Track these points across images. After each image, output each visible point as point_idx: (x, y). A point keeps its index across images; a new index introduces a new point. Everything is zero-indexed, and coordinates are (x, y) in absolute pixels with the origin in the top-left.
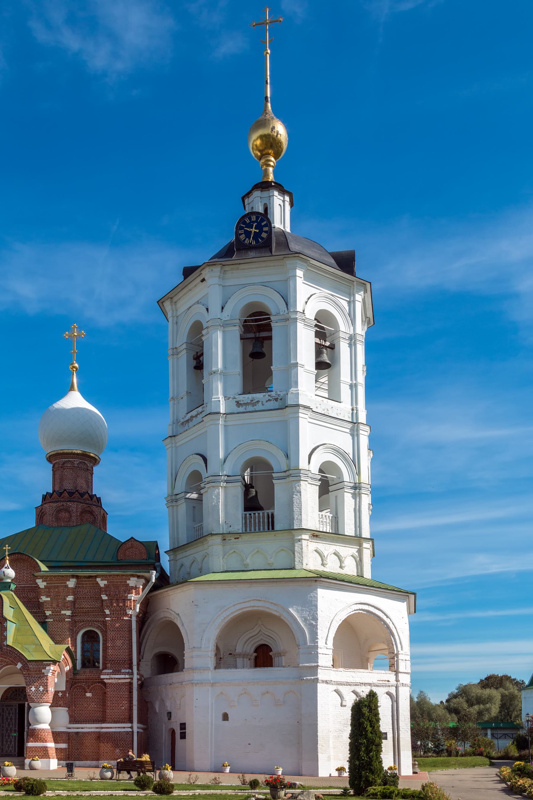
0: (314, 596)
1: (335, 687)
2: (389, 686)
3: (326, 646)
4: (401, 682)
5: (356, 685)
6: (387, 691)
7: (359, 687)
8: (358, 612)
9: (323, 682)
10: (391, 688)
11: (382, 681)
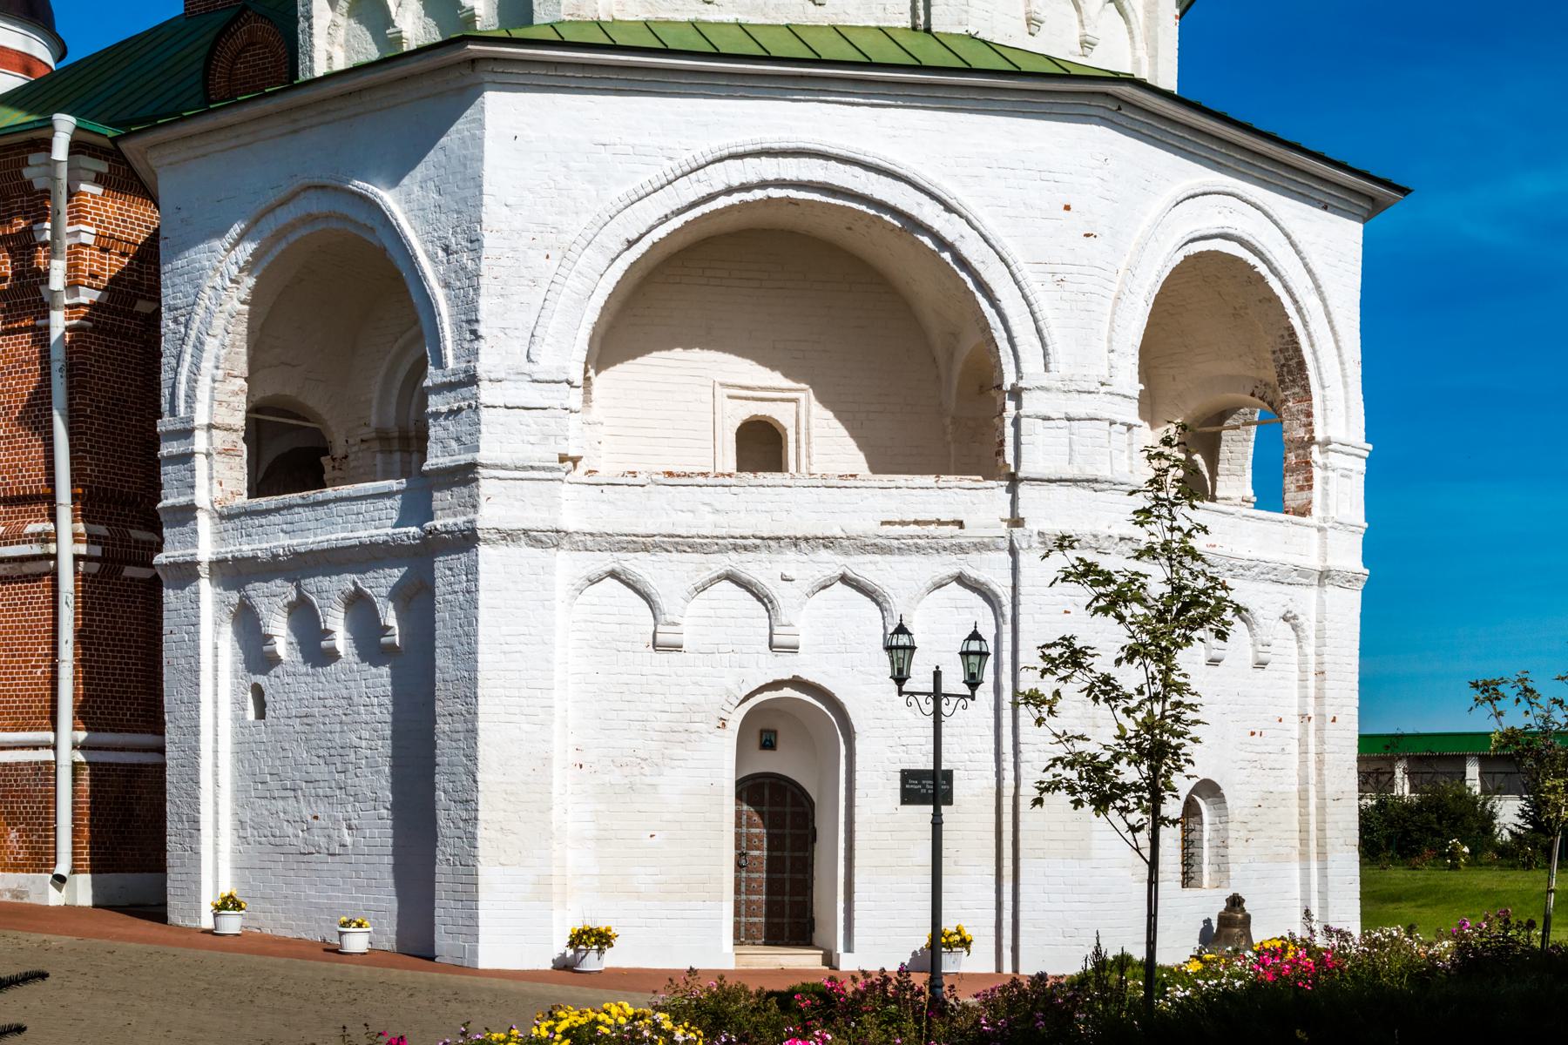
0: (473, 137)
1: (608, 561)
2: (962, 549)
3: (528, 368)
4: (1032, 526)
5: (740, 545)
6: (954, 571)
8: (759, 194)
9: (508, 536)
10: (974, 556)
11: (903, 523)
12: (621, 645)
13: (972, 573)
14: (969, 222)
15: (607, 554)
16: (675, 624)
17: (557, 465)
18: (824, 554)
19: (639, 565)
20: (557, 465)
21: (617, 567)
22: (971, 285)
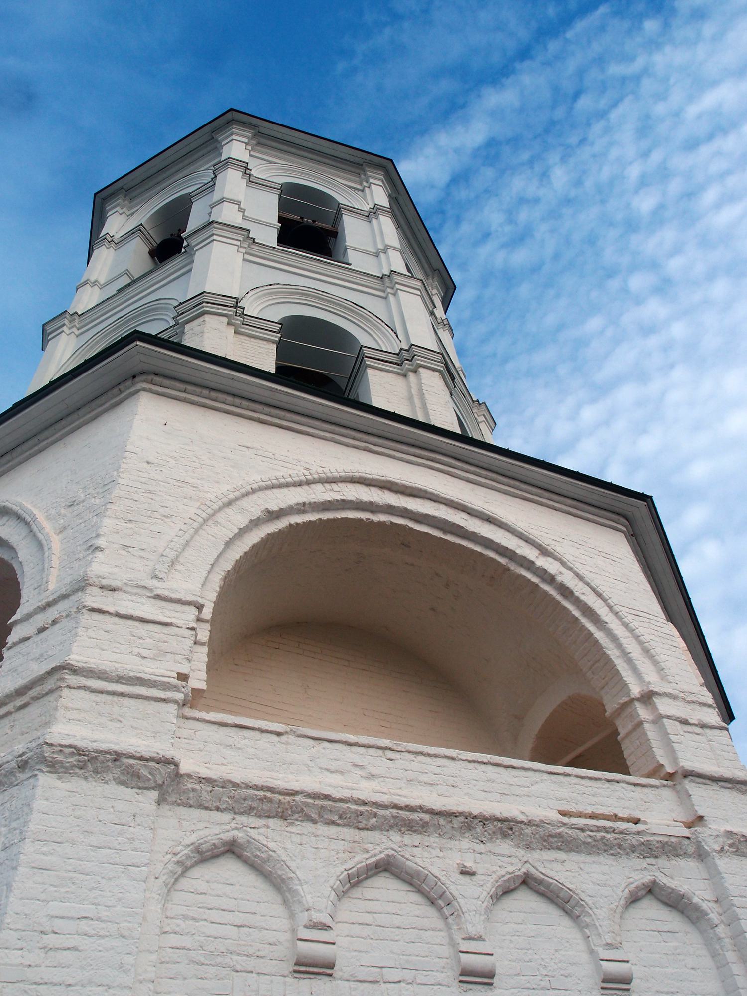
6: (647, 878)
7: (433, 840)
10: (662, 862)
12: (238, 961)
13: (663, 880)
14: (563, 563)
15: (226, 817)
16: (325, 927)
17: (175, 681)
18: (504, 846)
19: (271, 836)
20: (175, 681)
21: (239, 835)
22: (576, 613)
